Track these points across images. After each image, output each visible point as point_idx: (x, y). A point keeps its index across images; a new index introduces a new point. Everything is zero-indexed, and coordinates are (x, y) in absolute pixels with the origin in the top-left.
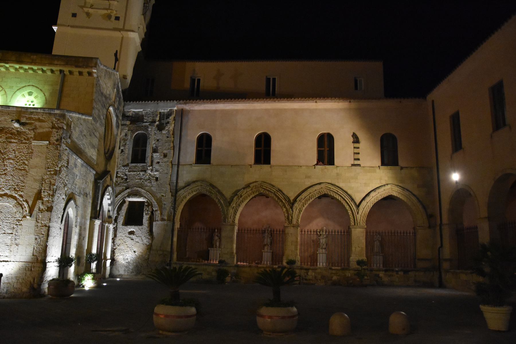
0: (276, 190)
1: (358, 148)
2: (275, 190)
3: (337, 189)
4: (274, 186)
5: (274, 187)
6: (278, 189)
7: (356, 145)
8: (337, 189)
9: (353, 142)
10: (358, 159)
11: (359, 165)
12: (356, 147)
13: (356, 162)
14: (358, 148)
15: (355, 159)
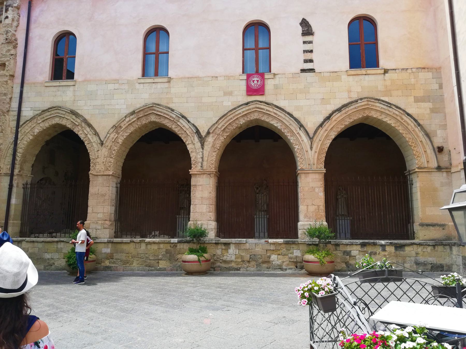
0: (177, 116)
1: (311, 42)
2: (174, 116)
3: (275, 111)
4: (173, 110)
5: (172, 112)
6: (180, 115)
7: (308, 38)
8: (275, 111)
9: (304, 34)
10: (311, 61)
11: (312, 70)
12: (307, 42)
13: (308, 66)
14: (311, 42)
15: (306, 61)
